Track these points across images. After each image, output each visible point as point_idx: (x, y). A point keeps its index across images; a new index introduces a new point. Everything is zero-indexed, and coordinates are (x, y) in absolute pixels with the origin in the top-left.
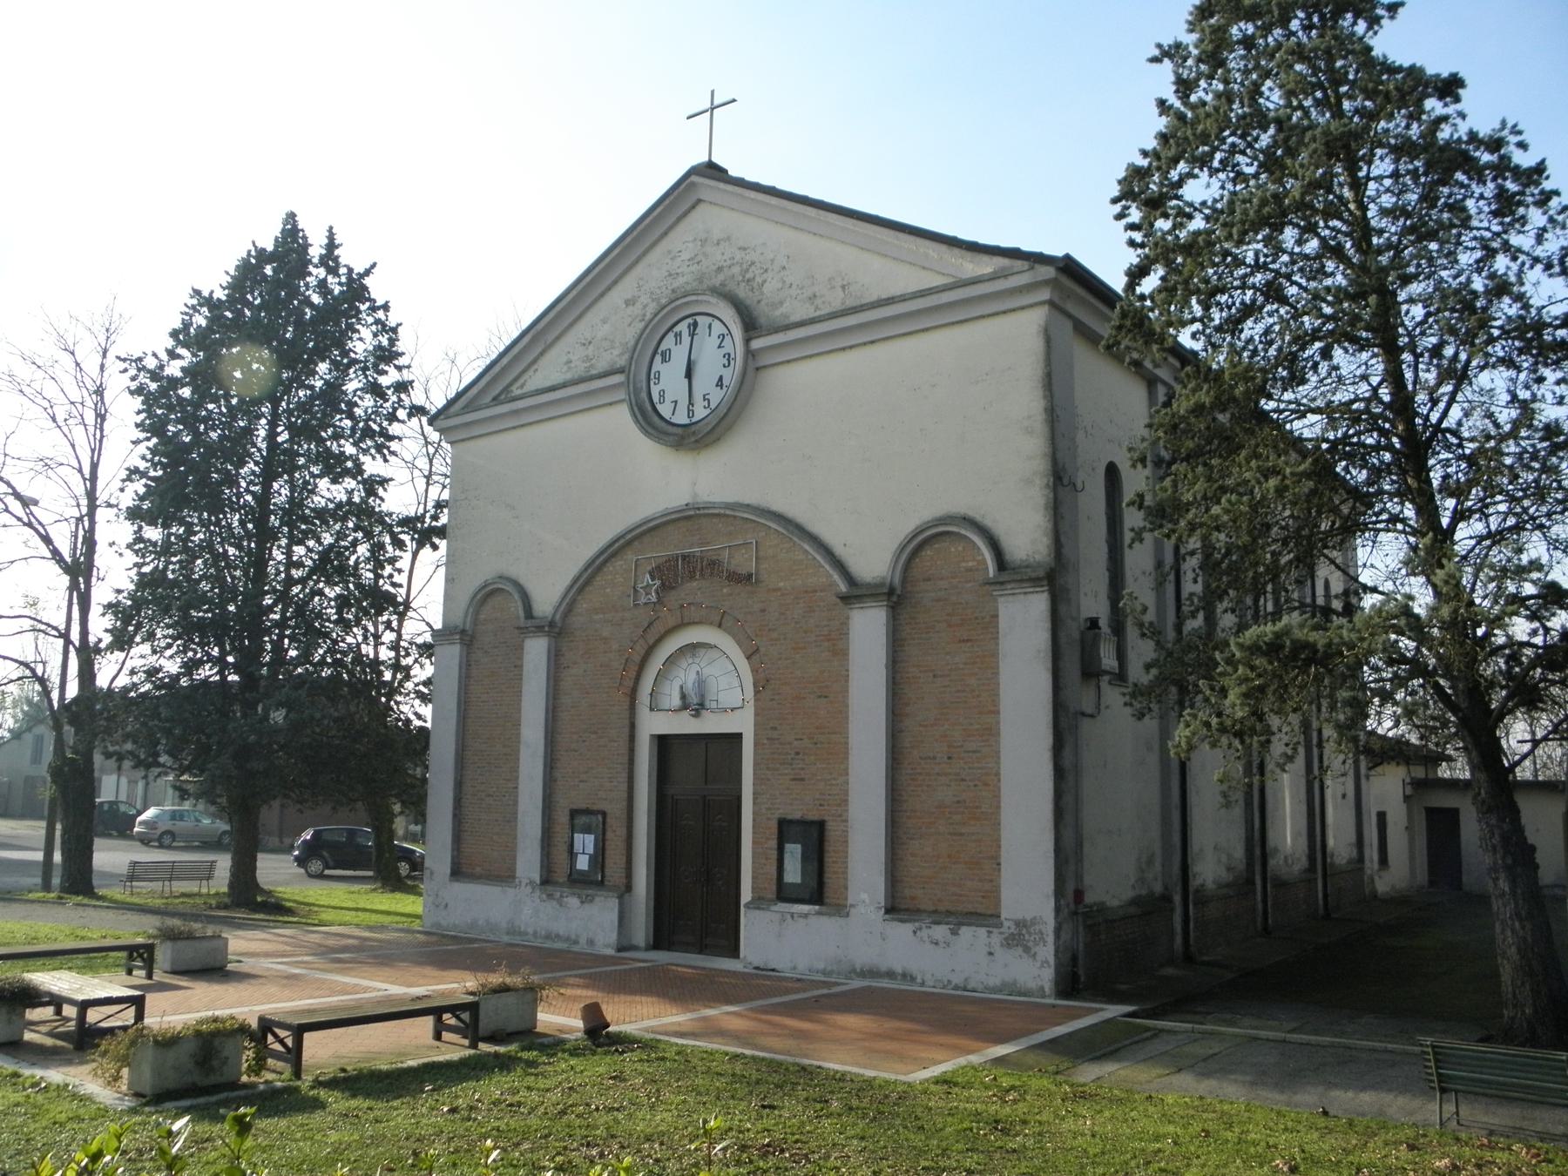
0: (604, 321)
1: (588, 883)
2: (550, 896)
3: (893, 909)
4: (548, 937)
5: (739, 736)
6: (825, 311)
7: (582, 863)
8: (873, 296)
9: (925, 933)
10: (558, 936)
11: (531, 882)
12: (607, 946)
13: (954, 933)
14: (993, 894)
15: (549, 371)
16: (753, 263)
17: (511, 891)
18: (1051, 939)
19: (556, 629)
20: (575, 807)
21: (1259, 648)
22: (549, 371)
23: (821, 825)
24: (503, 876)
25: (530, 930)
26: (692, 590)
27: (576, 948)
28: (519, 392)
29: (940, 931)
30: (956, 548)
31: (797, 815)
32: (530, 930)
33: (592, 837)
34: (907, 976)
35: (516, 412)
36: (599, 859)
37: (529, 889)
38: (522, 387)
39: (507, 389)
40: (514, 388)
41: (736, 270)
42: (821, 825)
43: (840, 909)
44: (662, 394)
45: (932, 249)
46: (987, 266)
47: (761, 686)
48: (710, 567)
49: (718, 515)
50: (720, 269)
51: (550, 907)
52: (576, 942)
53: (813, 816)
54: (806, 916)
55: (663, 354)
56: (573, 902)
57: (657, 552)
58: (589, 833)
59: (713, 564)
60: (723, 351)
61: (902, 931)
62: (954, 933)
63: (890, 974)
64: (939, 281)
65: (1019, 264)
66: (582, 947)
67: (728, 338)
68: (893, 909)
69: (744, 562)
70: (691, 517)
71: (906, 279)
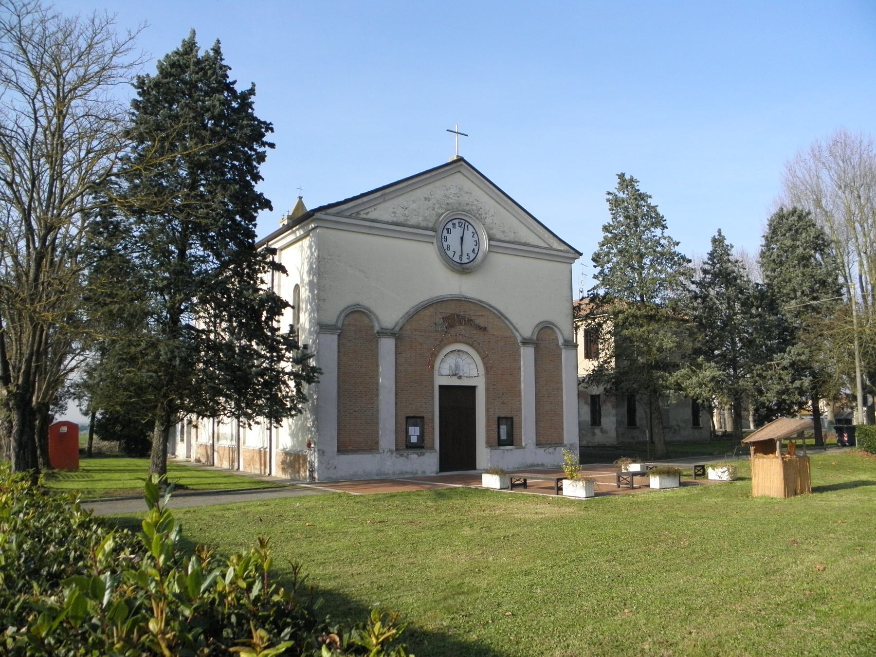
0: (414, 202)
1: (420, 446)
2: (402, 455)
3: (539, 444)
4: (401, 473)
5: (473, 389)
6: (507, 239)
7: (414, 440)
8: (523, 241)
9: (547, 451)
10: (406, 472)
11: (391, 451)
12: (433, 472)
13: (555, 449)
14: (561, 437)
15: (384, 212)
16: (481, 208)
17: (378, 456)
18: (578, 448)
19: (397, 334)
20: (408, 415)
21: (673, 366)
22: (384, 212)
23: (512, 418)
24: (371, 446)
25: (391, 472)
26: (460, 329)
27: (417, 475)
28: (365, 216)
29: (551, 450)
30: (550, 331)
31: (503, 416)
32: (391, 472)
33: (418, 428)
34: (543, 465)
35: (370, 227)
36: (421, 437)
37: (389, 453)
38: (367, 214)
39: (358, 213)
40: (362, 213)
41: (474, 207)
42: (512, 418)
43: (520, 447)
44: (448, 246)
45: (547, 235)
46: (563, 247)
47: (488, 369)
48: (469, 322)
49: (474, 303)
50: (468, 204)
51: (402, 460)
52: (416, 473)
53: (509, 415)
54: (511, 450)
55: (448, 229)
56: (414, 456)
57: (452, 309)
58: (417, 426)
59: (470, 320)
60: (474, 239)
61: (541, 451)
62: (555, 449)
63: (538, 465)
64: (543, 245)
65: (572, 251)
66: (420, 474)
67: (475, 235)
68: (539, 444)
69: (481, 322)
70: (461, 300)
71: (533, 240)
